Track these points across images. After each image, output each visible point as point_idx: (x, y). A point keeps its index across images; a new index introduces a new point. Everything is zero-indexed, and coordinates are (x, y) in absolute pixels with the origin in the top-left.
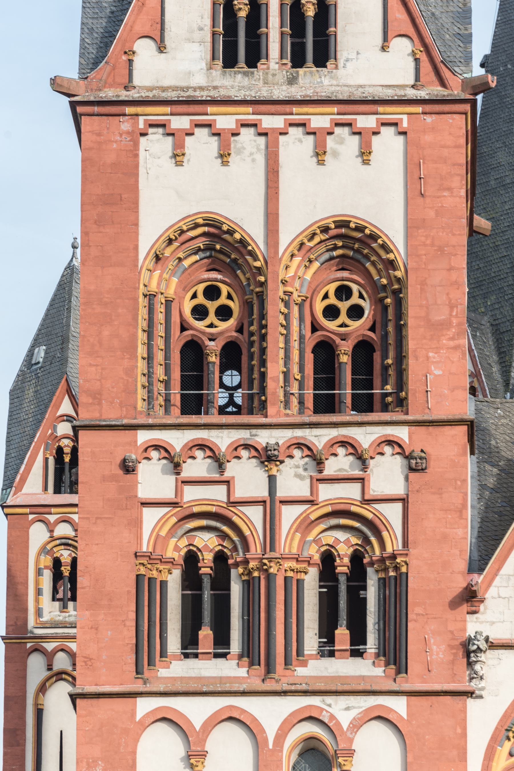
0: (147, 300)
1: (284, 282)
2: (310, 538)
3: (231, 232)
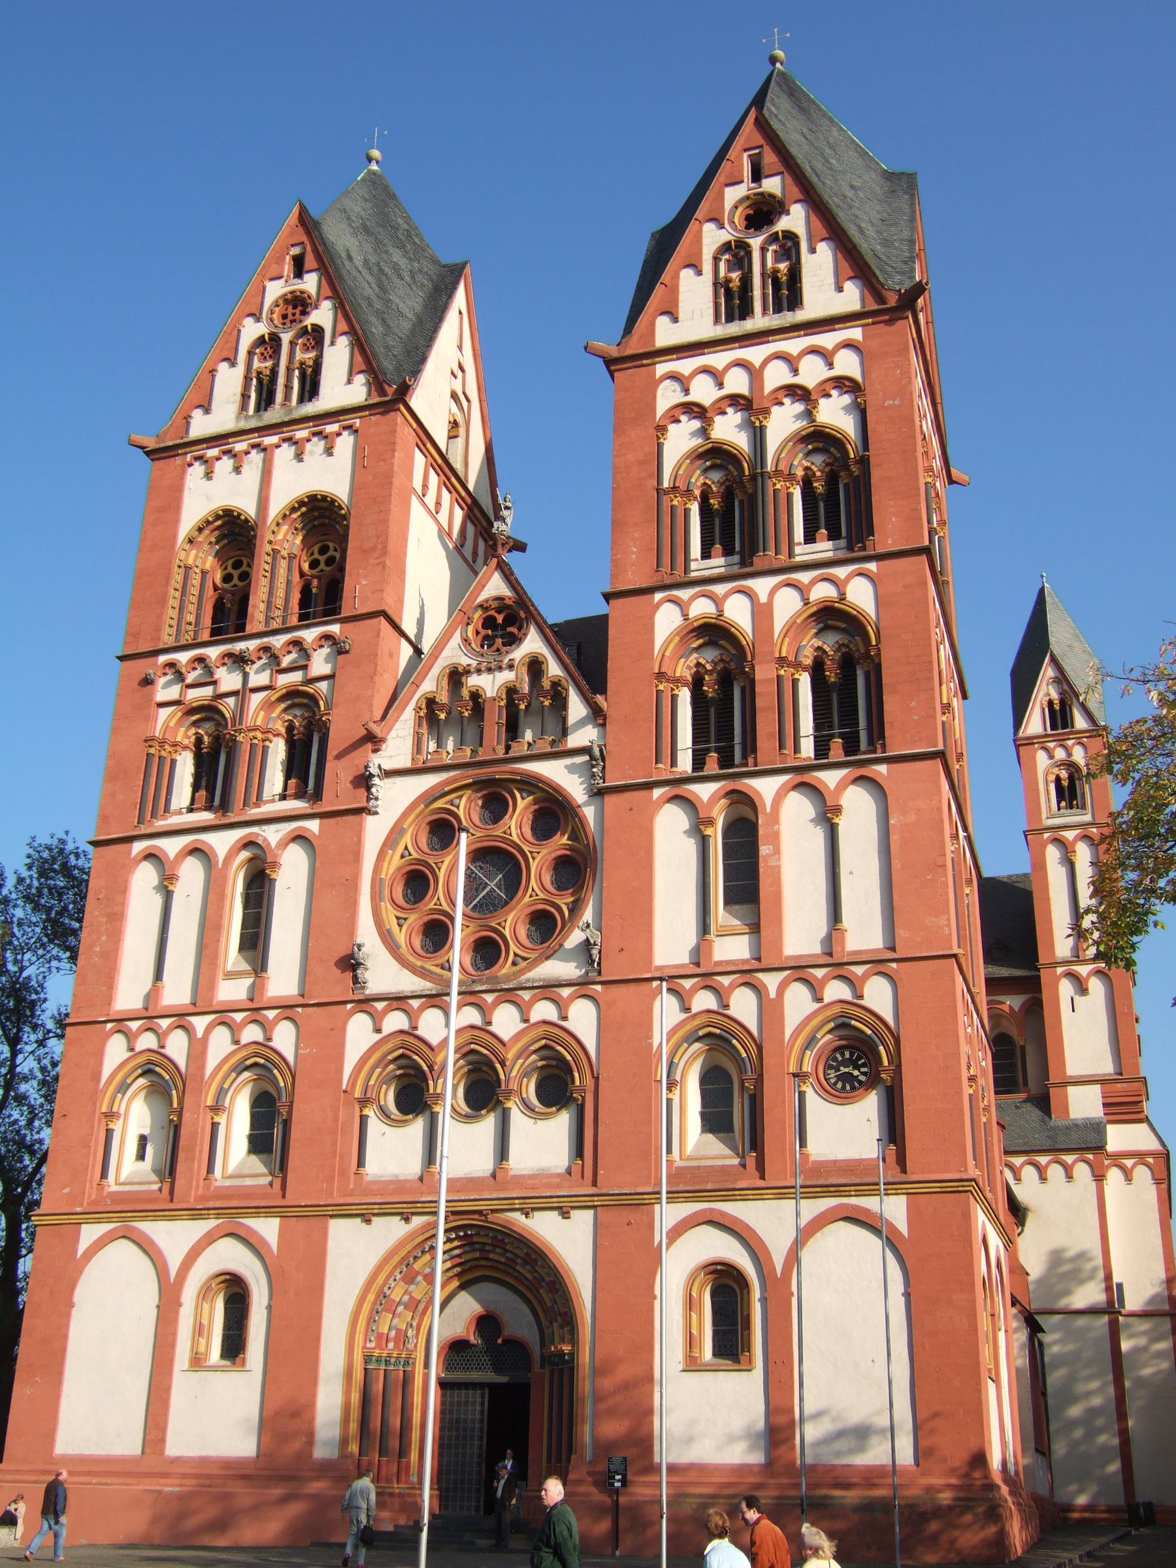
0: (182, 571)
1: (270, 542)
2: (274, 715)
3: (239, 514)
